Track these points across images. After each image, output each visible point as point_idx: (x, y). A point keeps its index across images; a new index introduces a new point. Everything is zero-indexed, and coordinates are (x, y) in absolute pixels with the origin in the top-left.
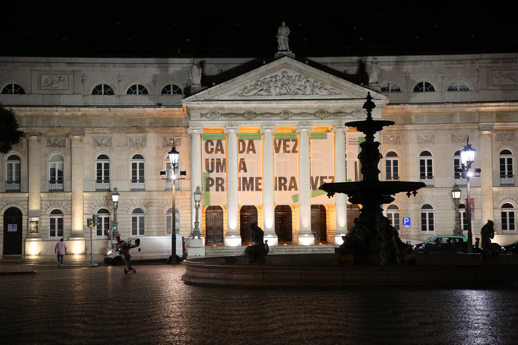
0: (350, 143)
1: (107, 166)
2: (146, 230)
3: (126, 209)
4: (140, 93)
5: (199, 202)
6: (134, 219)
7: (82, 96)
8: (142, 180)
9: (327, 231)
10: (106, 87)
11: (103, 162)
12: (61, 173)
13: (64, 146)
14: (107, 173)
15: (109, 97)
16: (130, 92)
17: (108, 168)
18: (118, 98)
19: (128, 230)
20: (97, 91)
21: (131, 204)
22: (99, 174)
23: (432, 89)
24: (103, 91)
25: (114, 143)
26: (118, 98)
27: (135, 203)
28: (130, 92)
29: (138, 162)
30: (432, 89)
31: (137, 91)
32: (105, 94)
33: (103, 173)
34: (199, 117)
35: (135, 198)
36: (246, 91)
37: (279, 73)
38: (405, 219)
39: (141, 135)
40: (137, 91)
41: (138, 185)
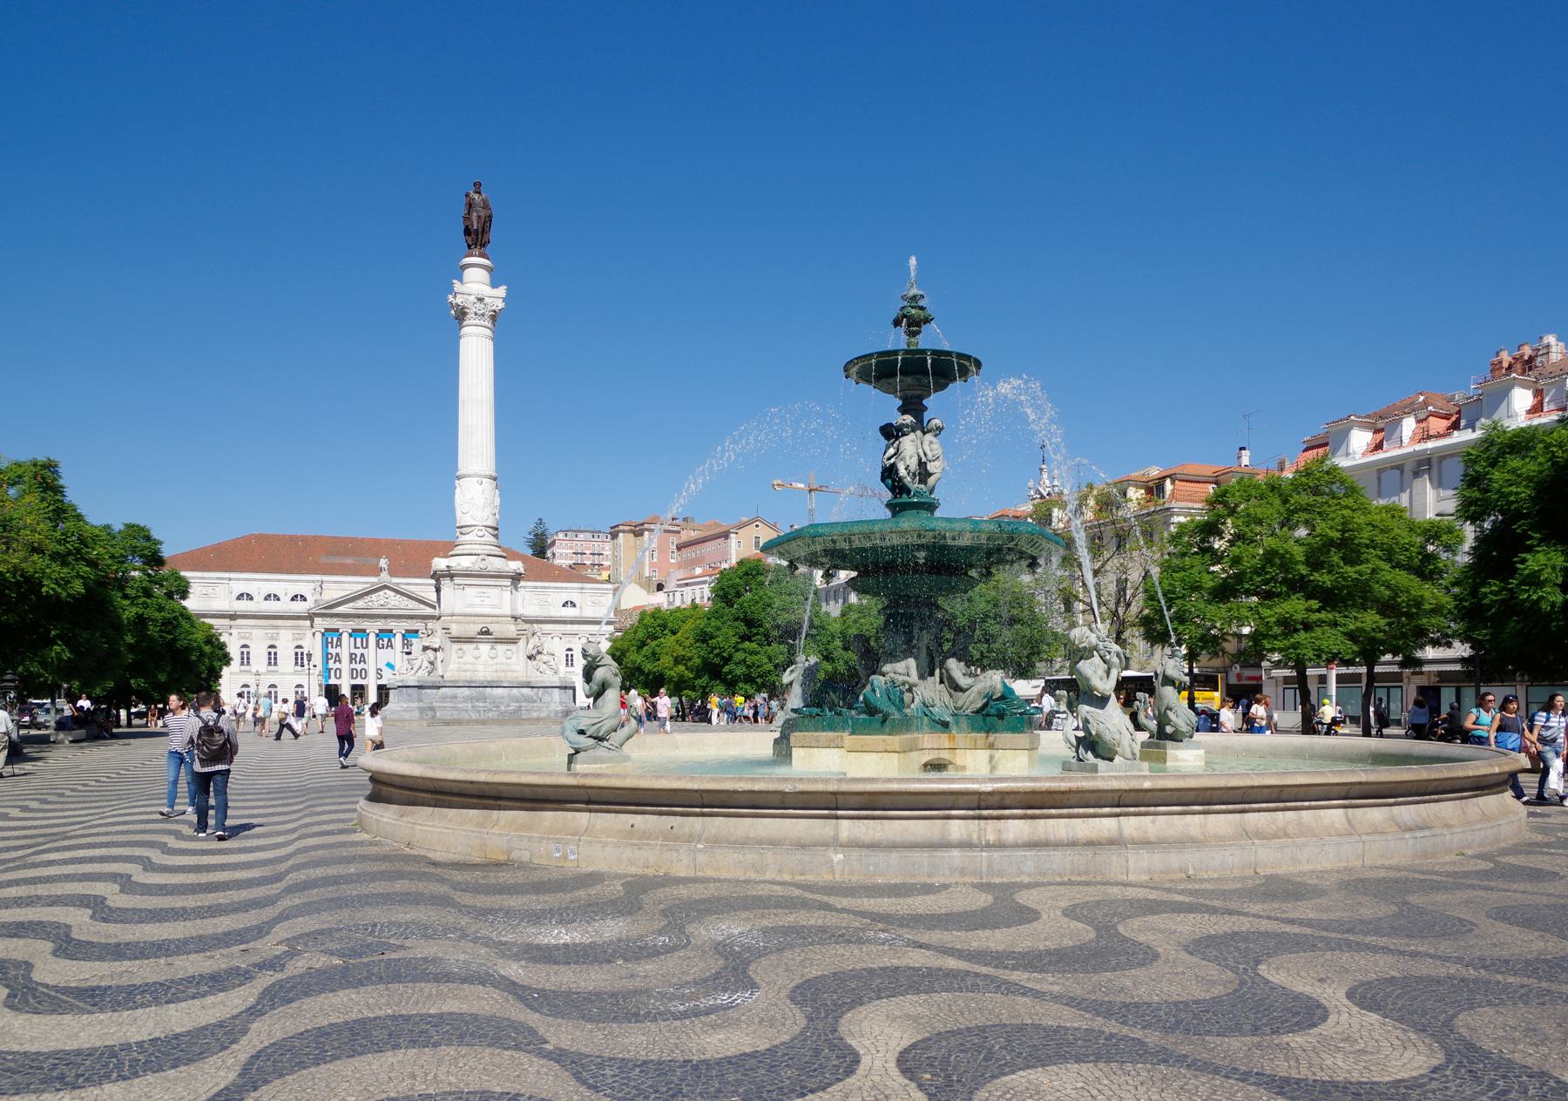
20: (240, 597)
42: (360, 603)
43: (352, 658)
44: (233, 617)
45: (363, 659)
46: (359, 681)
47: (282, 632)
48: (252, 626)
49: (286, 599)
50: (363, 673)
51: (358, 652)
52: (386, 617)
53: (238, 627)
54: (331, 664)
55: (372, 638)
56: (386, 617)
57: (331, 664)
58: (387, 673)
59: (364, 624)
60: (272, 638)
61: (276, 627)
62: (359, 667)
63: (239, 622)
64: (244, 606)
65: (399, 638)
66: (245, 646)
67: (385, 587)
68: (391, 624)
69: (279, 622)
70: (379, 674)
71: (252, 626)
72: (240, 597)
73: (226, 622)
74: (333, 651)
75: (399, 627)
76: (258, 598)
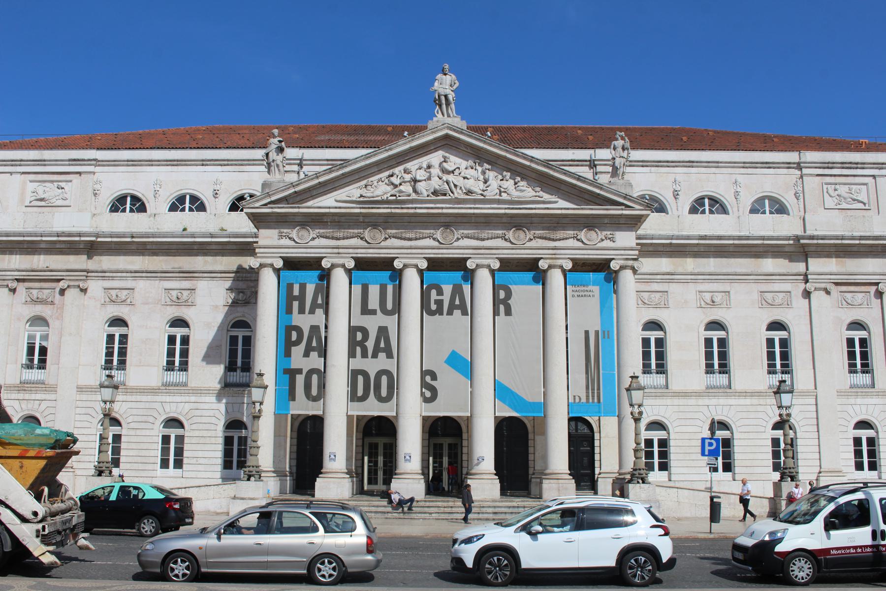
0: (576, 294)
1: (124, 338)
2: (185, 461)
3: (151, 419)
4: (191, 210)
5: (261, 403)
6: (166, 439)
7: (89, 215)
8: (184, 366)
9: (531, 471)
10: (135, 199)
11: (117, 331)
12: (43, 351)
13: (52, 303)
14: (123, 352)
15: (136, 215)
16: (173, 208)
17: (126, 343)
18: (152, 218)
19: (152, 460)
20: (118, 205)
21: (161, 410)
22: (109, 354)
23: (724, 210)
24: (128, 206)
25: (138, 297)
26: (152, 218)
27: (167, 410)
28: (173, 208)
29: (179, 332)
30: (724, 210)
31: (187, 205)
32: (132, 211)
33: (117, 353)
34: (276, 237)
35: (168, 399)
36: (369, 188)
37: (435, 158)
38: (707, 441)
39: (186, 284)
40: (187, 205)
41: (176, 376)
42: (379, 188)
43: (357, 340)
44: (92, 248)
45: (385, 345)
46: (373, 408)
47: (202, 285)
48: (137, 274)
49: (219, 206)
50: (386, 385)
51: (372, 324)
52: (450, 222)
53: (103, 274)
54: (298, 359)
55: (412, 283)
56: (450, 222)
57: (298, 359)
58: (448, 380)
59: (386, 245)
60: (178, 302)
61: (188, 274)
62: (372, 366)
63: (106, 262)
64: (128, 223)
65: (484, 280)
66: (119, 322)
67: (448, 143)
68: (461, 245)
69: (199, 262)
70: (430, 393)
71: (137, 274)
72: (118, 205)
73: (78, 261)
74: (305, 322)
75: (483, 250)
76: (158, 205)
